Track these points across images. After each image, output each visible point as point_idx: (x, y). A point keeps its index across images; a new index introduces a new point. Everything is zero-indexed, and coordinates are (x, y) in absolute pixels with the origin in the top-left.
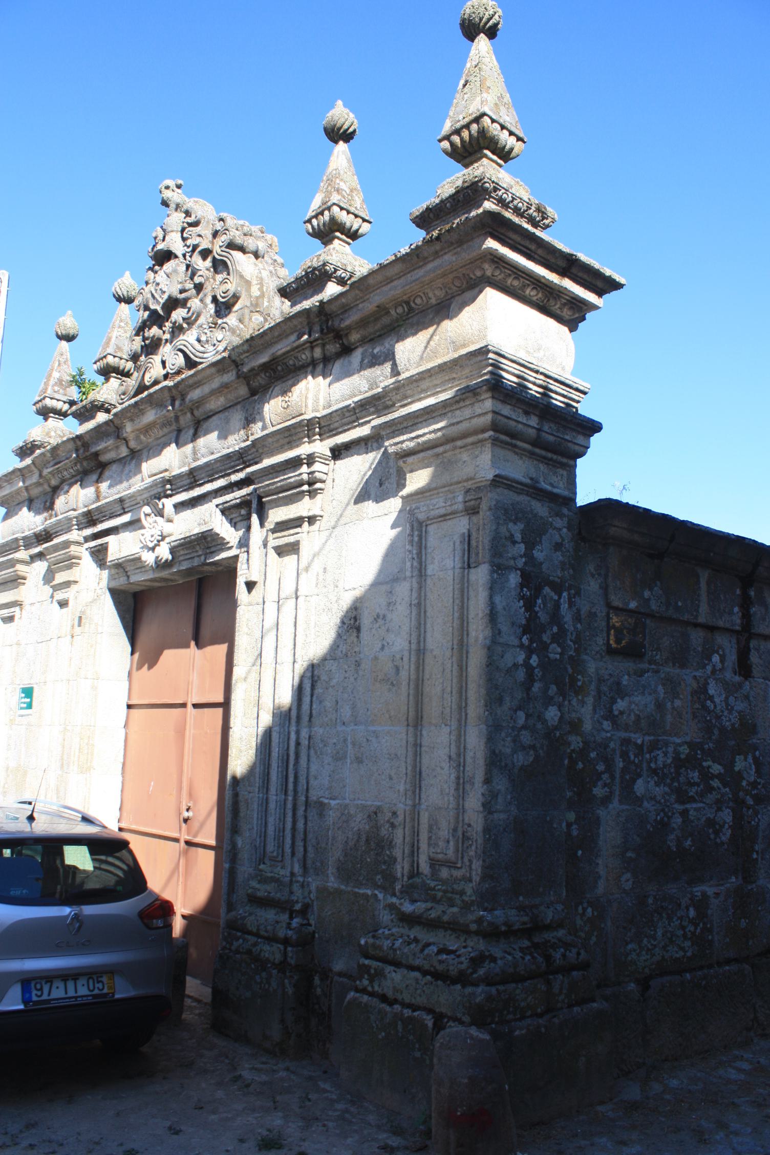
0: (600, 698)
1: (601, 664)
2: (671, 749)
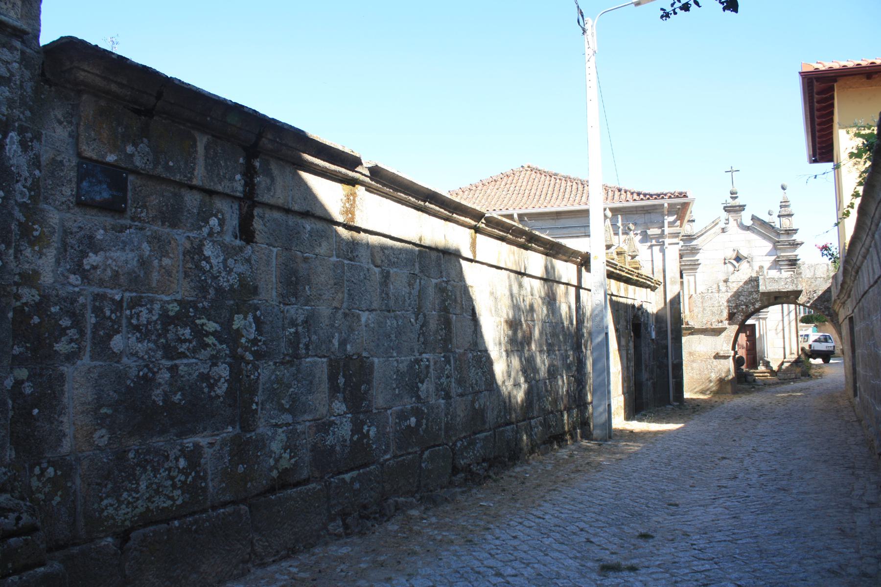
0: (66, 251)
1: (69, 215)
2: (157, 306)
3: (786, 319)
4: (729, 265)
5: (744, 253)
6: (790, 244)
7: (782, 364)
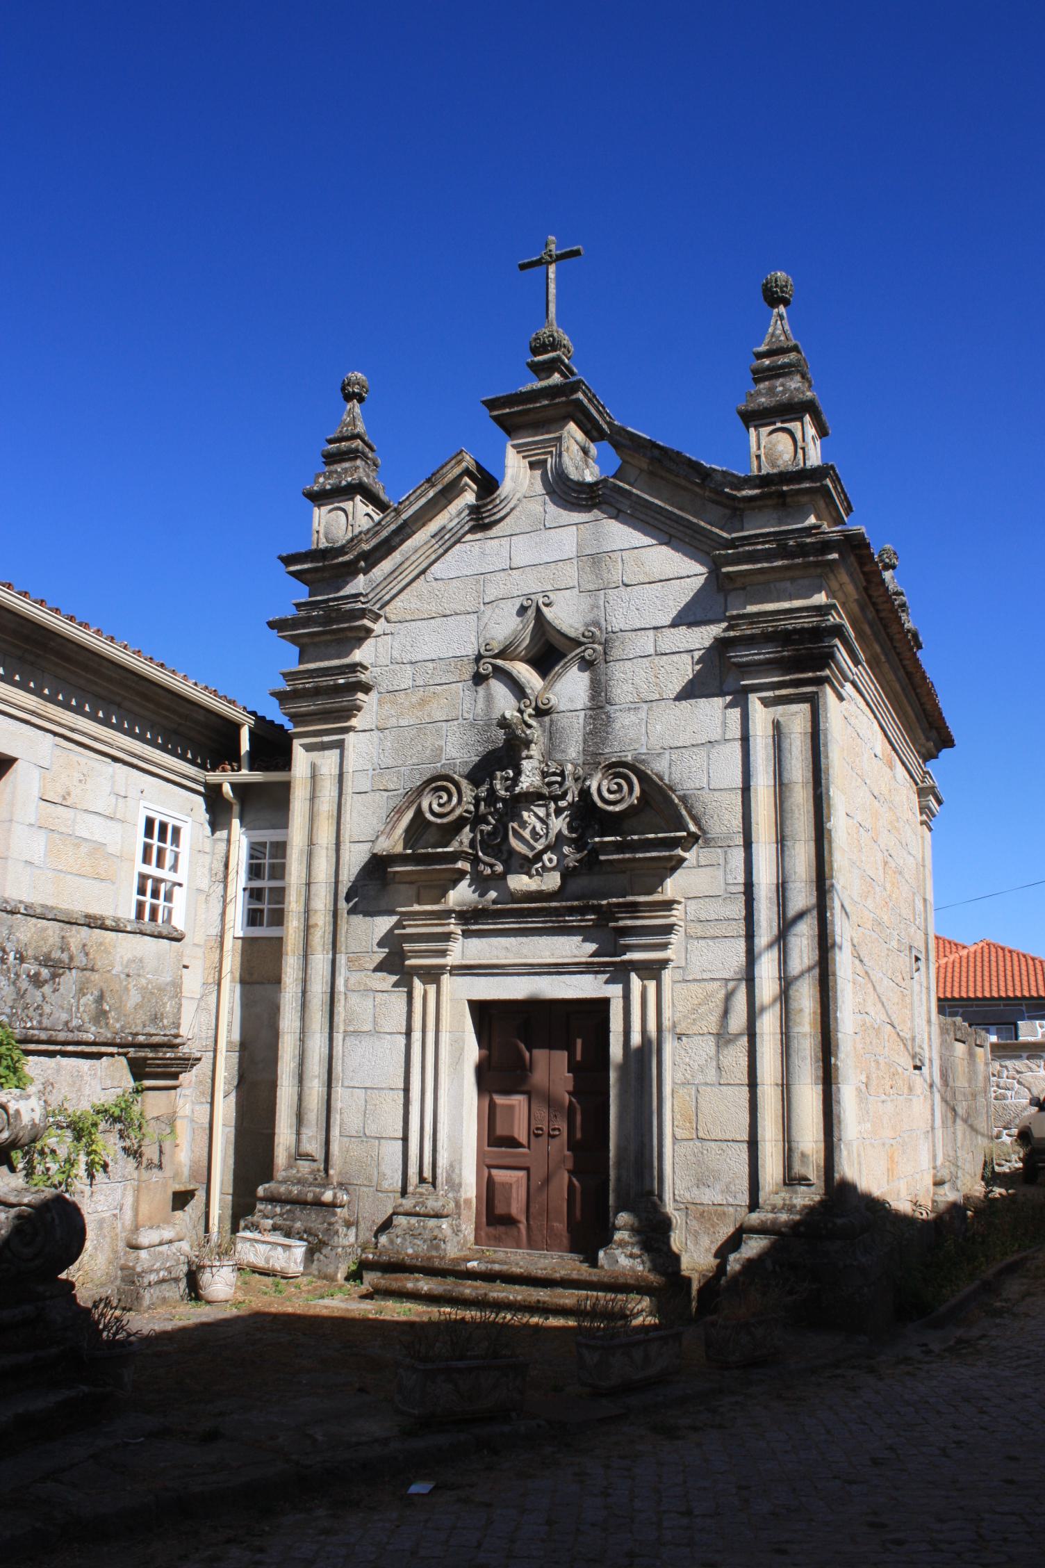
3: (767, 969)
4: (498, 688)
5: (567, 616)
6: (783, 551)
7: (734, 1242)
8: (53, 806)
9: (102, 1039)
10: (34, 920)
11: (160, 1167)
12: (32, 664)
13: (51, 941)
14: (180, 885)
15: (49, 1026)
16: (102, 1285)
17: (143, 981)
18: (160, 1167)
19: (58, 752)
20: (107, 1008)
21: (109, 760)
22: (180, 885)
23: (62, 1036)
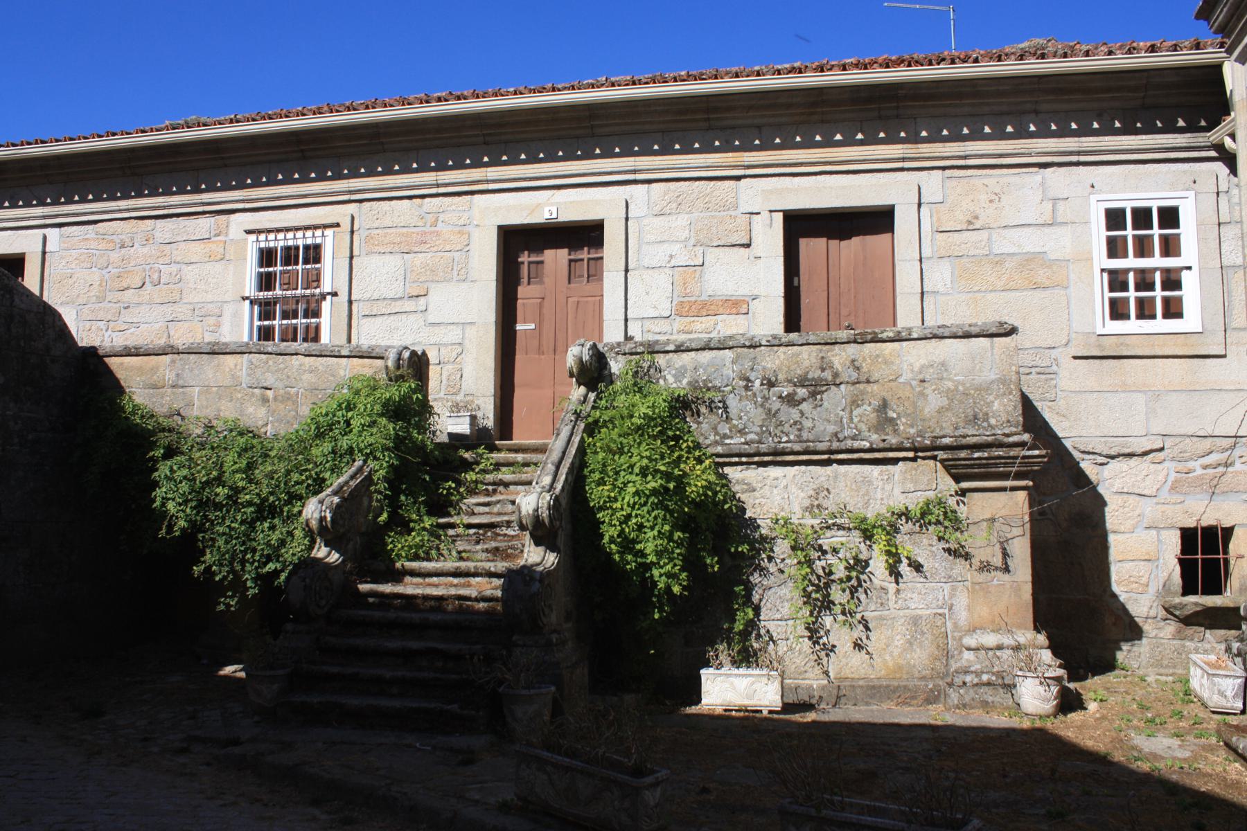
8: (956, 234)
9: (882, 445)
10: (782, 349)
11: (1006, 569)
12: (898, 117)
13: (807, 363)
14: (1189, 268)
15: (811, 438)
16: (923, 678)
17: (950, 384)
18: (1006, 569)
19: (954, 183)
20: (895, 415)
21: (1036, 169)
22: (1189, 268)
23: (822, 446)
